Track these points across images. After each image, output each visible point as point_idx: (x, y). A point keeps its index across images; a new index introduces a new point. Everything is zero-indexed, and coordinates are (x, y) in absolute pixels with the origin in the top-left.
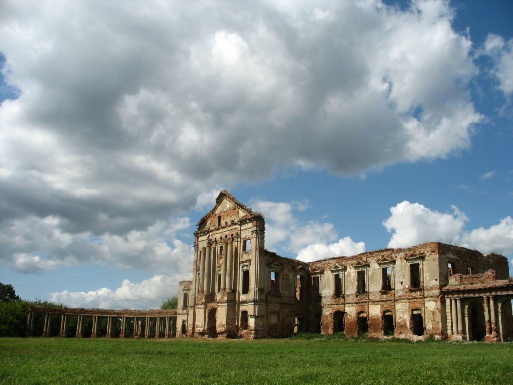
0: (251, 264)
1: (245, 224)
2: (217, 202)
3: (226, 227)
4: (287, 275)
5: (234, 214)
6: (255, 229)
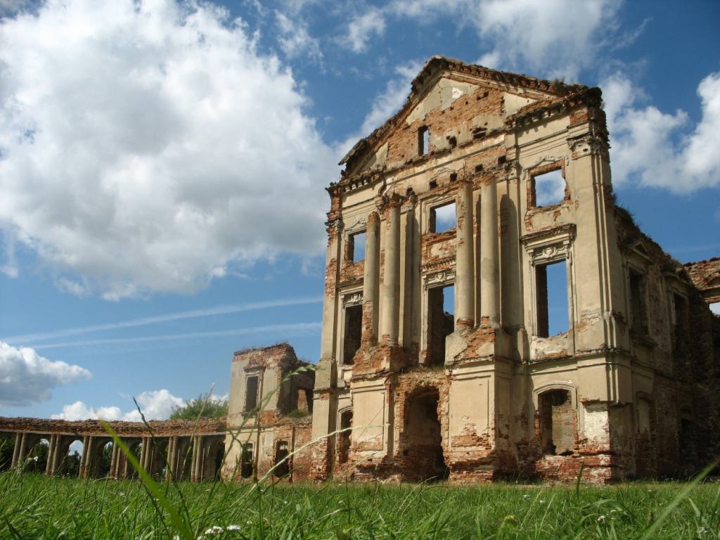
0: (572, 239)
1: (535, 126)
2: (414, 89)
3: (450, 152)
4: (655, 288)
6: (587, 130)
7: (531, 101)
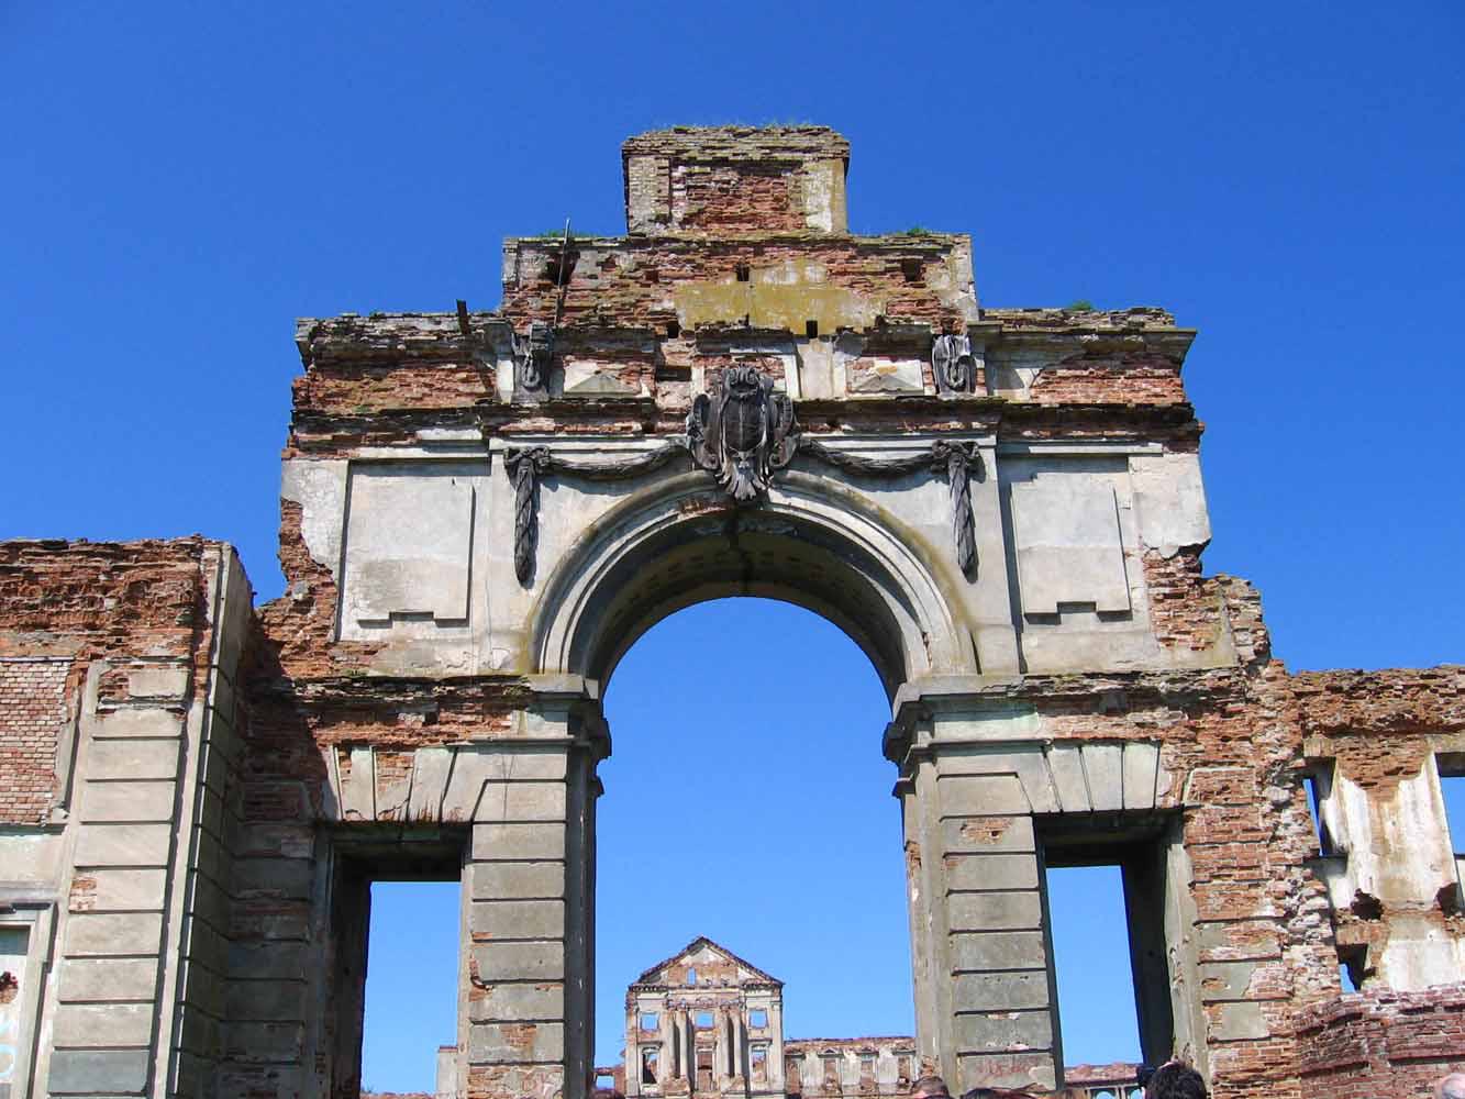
5: (723, 973)
7: (752, 977)
